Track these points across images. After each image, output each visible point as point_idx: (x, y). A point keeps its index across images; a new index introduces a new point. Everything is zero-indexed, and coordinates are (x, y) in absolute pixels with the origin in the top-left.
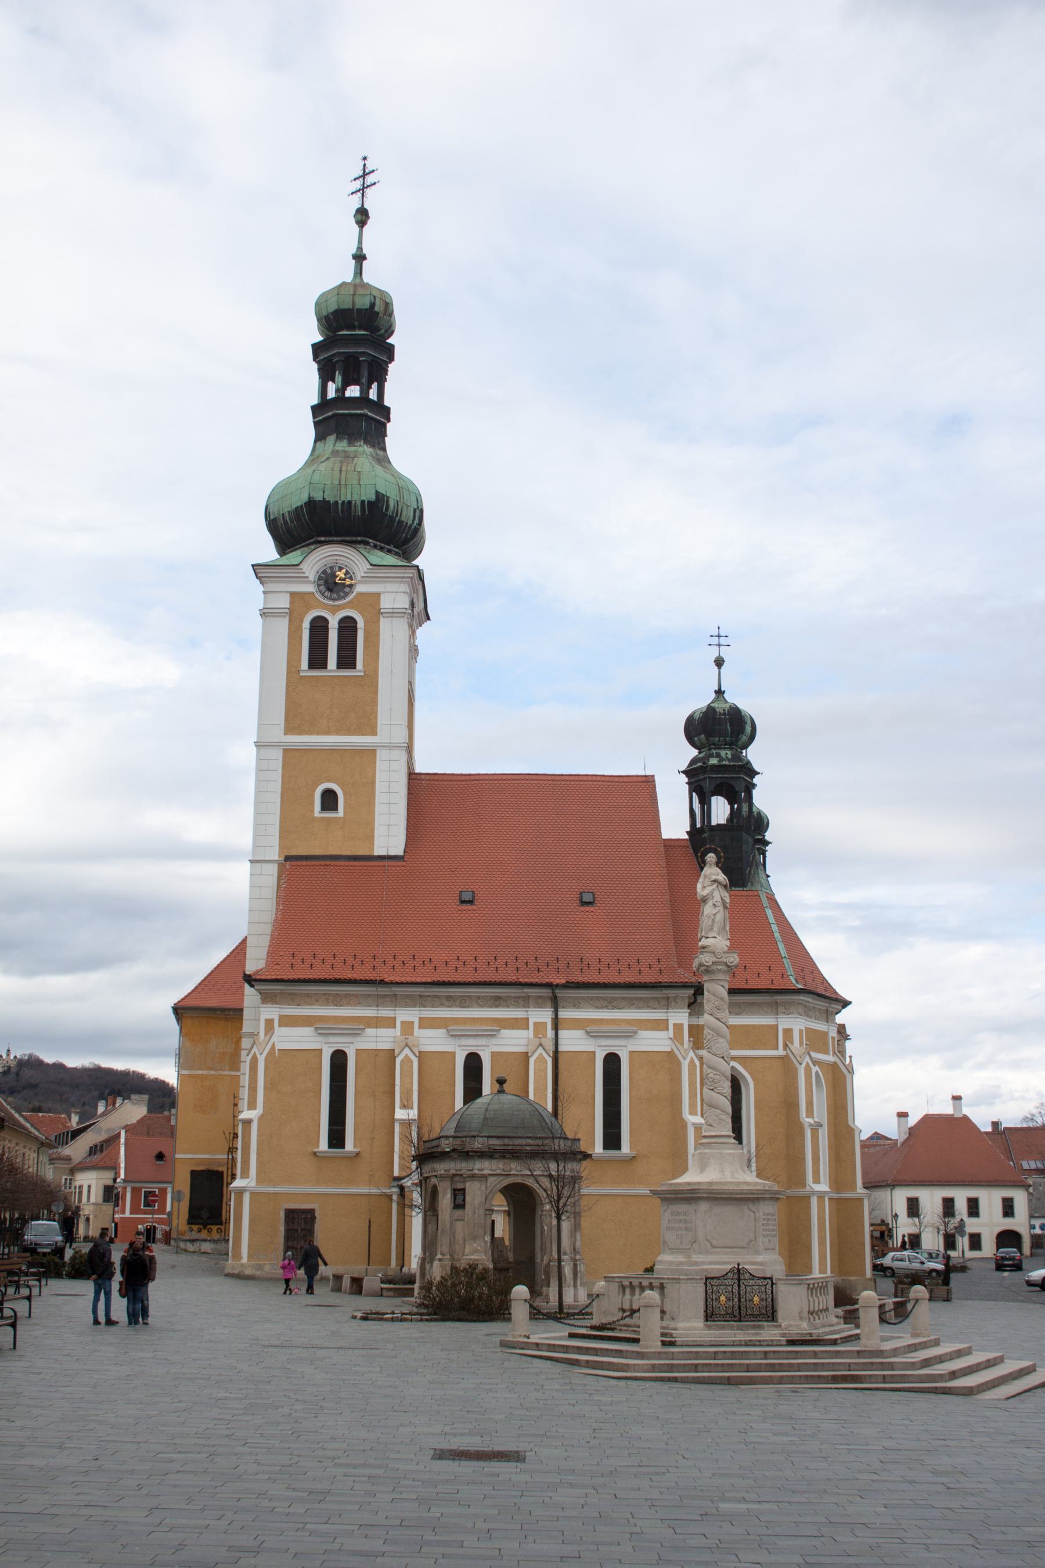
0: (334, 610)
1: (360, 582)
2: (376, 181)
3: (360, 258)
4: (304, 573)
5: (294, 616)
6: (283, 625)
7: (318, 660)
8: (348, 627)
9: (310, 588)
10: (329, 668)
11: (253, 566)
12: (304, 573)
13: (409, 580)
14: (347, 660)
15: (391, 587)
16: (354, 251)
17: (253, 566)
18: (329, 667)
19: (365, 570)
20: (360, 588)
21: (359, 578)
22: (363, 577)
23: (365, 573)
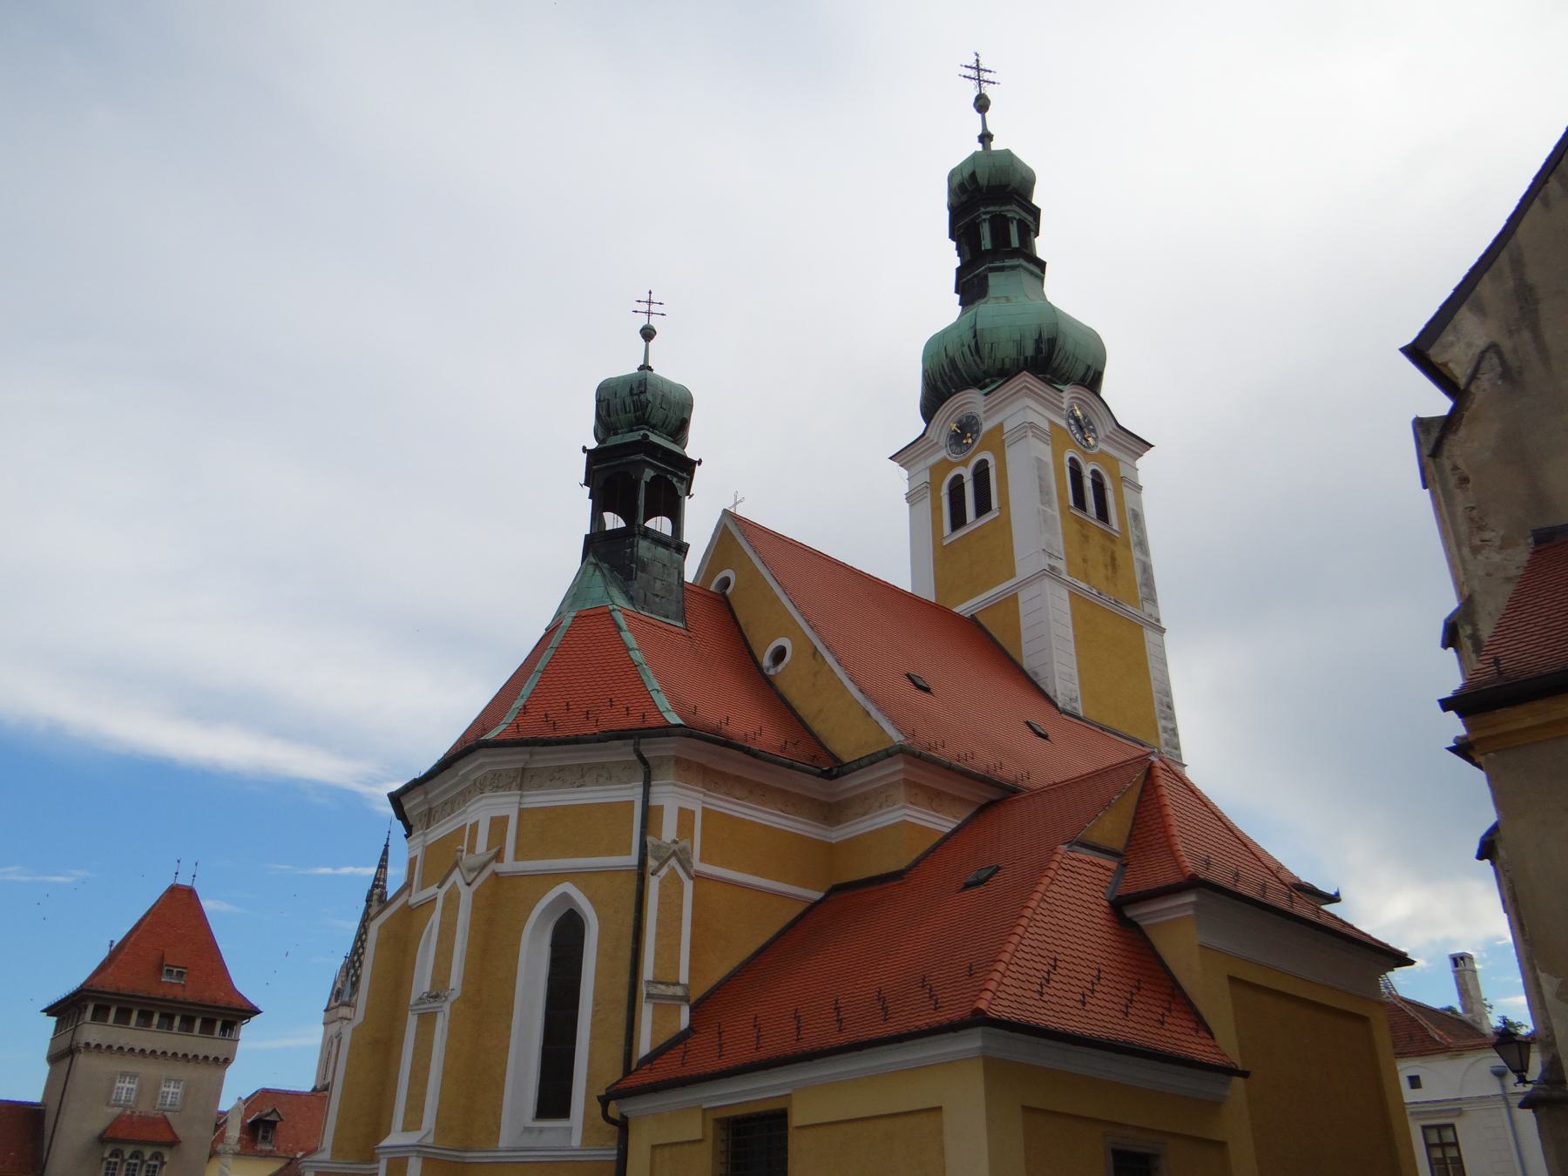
0: (965, 463)
1: (986, 419)
2: (976, 58)
3: (985, 138)
4: (932, 441)
5: (934, 486)
6: (926, 505)
7: (958, 520)
8: (981, 474)
9: (943, 454)
10: (968, 522)
11: (891, 458)
12: (932, 441)
13: (1025, 391)
14: (983, 506)
15: (1009, 410)
16: (979, 132)
17: (891, 458)
18: (968, 521)
19: (984, 403)
20: (986, 426)
21: (982, 416)
22: (985, 412)
23: (986, 406)
